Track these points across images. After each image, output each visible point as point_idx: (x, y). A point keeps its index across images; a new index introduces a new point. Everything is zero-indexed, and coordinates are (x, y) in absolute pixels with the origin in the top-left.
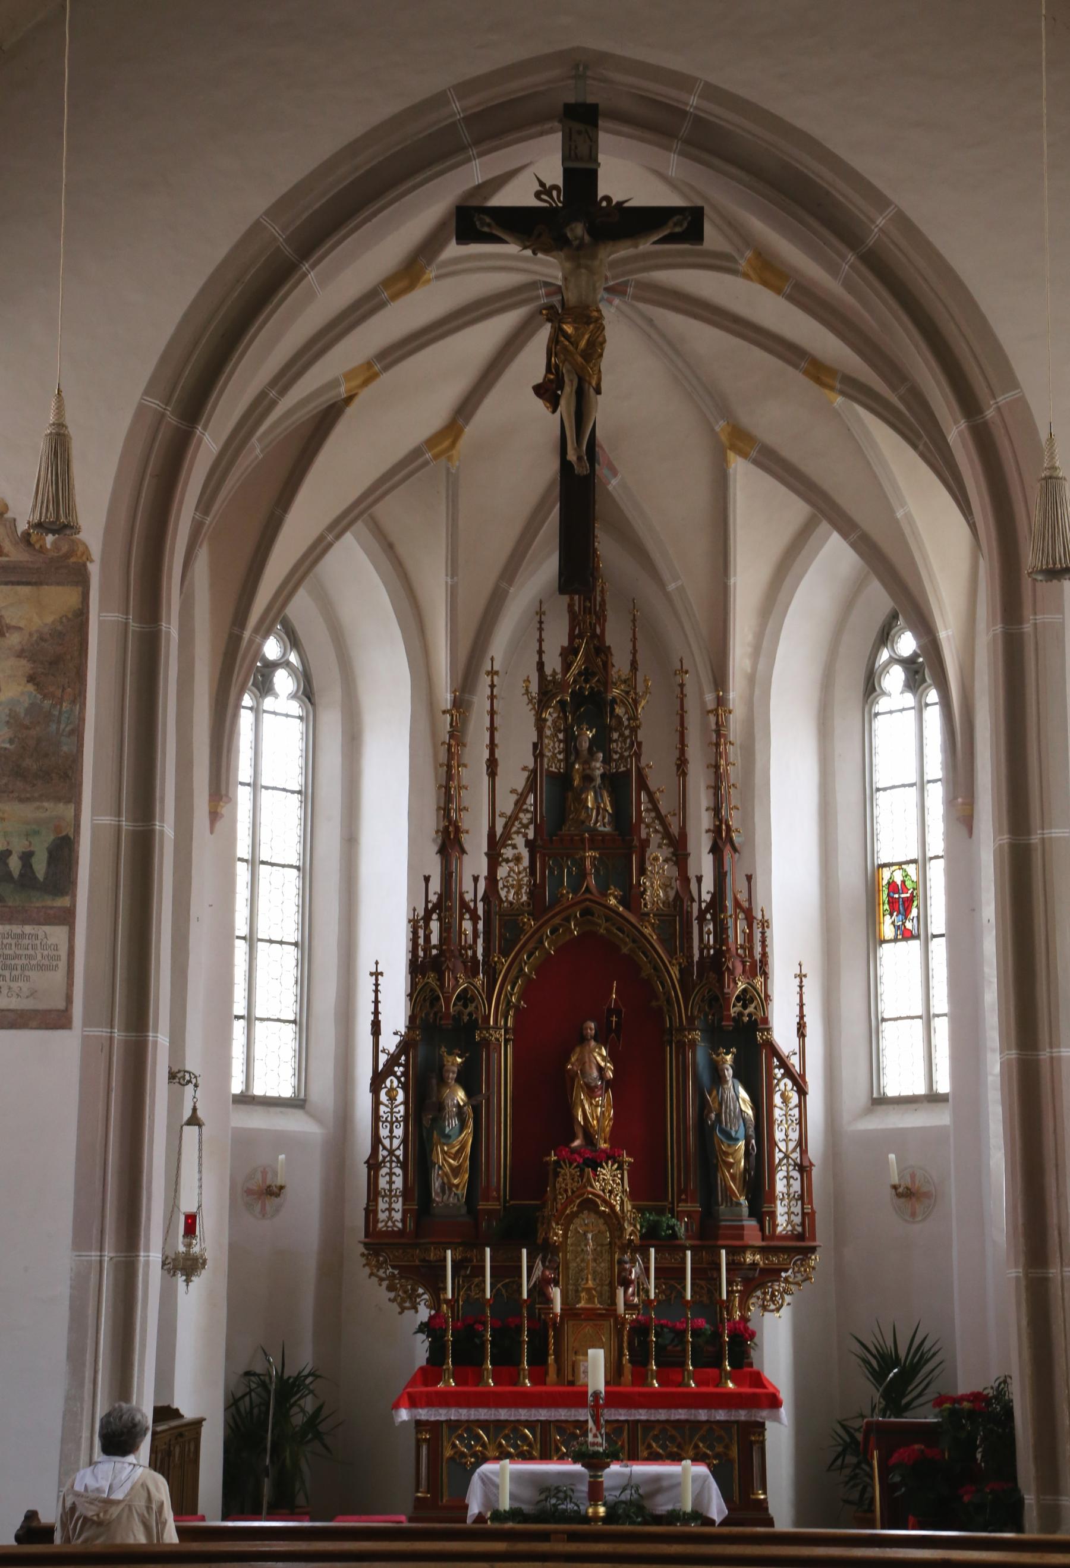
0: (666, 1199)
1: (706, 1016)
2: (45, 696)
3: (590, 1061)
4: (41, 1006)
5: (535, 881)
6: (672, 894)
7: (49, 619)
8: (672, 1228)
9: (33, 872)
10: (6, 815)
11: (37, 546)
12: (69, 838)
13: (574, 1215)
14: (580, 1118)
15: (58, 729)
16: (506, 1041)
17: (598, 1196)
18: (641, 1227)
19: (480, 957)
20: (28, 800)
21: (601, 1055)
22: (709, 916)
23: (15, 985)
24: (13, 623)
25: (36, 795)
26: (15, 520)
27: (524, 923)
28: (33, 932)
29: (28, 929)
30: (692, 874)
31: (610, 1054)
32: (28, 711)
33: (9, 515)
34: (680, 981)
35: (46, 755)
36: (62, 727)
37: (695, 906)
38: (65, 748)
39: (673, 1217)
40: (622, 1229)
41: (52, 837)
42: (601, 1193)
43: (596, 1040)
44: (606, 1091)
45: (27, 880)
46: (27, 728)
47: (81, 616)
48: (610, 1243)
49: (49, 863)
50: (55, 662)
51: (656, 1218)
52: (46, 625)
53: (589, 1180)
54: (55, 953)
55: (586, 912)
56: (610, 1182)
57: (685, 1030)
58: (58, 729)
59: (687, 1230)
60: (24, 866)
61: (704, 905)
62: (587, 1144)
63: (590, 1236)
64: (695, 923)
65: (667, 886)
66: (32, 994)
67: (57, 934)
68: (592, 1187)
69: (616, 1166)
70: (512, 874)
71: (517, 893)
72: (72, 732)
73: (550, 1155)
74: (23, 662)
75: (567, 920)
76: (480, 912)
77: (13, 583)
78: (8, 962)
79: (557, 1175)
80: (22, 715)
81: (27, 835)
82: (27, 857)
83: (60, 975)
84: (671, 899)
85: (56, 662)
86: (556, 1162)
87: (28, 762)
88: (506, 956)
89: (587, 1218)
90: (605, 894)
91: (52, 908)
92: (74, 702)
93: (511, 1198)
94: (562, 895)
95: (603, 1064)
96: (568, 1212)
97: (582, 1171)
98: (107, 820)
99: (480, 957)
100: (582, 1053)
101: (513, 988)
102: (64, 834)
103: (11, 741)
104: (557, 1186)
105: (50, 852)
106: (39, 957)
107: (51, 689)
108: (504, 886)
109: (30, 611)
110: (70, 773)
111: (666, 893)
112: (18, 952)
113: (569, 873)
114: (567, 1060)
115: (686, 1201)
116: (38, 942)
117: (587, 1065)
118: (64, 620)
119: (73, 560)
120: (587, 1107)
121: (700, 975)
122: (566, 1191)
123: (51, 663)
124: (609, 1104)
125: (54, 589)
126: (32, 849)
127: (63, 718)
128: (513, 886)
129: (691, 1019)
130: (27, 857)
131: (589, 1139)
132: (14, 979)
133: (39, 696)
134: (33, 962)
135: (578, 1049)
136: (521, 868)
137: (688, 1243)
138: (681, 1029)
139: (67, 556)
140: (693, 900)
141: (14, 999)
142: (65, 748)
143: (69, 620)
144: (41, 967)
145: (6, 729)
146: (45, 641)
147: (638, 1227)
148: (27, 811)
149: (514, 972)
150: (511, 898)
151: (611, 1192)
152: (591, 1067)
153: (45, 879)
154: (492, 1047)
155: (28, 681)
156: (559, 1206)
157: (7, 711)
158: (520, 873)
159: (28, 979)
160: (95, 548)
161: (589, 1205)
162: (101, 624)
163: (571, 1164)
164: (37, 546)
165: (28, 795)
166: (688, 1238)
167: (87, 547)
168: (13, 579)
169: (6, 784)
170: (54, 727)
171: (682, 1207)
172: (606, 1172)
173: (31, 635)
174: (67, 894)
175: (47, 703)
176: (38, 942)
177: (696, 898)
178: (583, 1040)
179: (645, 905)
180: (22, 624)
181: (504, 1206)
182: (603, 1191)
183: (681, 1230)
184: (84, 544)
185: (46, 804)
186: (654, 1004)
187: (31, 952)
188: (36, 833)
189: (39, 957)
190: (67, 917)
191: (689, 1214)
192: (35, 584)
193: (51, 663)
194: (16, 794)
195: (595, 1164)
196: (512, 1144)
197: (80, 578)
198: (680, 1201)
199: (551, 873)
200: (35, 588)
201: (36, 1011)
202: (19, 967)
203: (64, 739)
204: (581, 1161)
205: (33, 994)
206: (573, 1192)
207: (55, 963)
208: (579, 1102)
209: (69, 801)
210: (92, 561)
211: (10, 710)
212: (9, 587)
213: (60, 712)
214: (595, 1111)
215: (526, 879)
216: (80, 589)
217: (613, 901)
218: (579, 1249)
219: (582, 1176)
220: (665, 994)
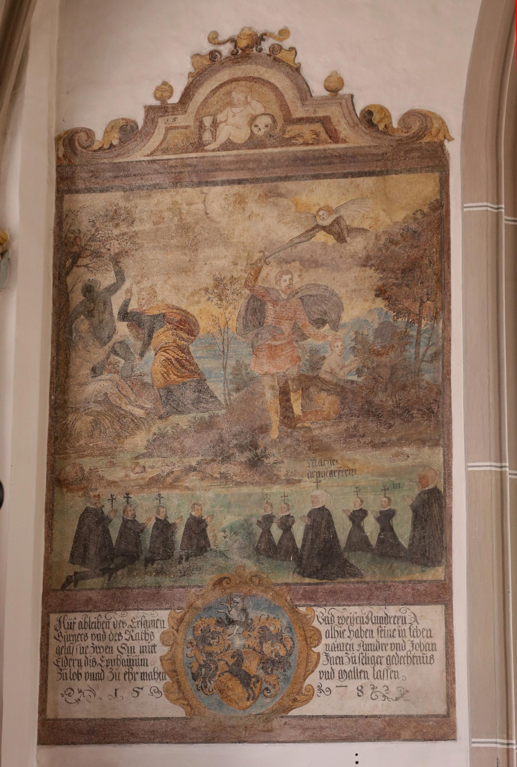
2: (399, 313)
4: (414, 711)
7: (400, 216)
9: (395, 537)
10: (357, 466)
11: (381, 127)
12: (439, 492)
15: (417, 354)
20: (383, 444)
23: (379, 683)
24: (356, 225)
25: (394, 438)
26: (352, 96)
28: (398, 614)
29: (392, 610)
32: (379, 333)
33: (345, 91)
35: (404, 387)
36: (422, 350)
38: (427, 377)
41: (417, 491)
45: (387, 548)
46: (379, 354)
47: (440, 208)
49: (414, 526)
50: (410, 269)
52: (396, 223)
54: (429, 641)
58: (417, 354)
60: (382, 530)
66: (402, 695)
67: (430, 616)
72: (435, 356)
74: (370, 271)
77: (353, 175)
78: (370, 654)
80: (372, 338)
81: (385, 489)
82: (386, 518)
83: (436, 669)
85: (412, 269)
87: (380, 398)
91: (421, 582)
92: (435, 318)
98: (487, 466)
102: (431, 486)
103: (359, 372)
105: (415, 510)
106: (409, 647)
107: (407, 303)
109: (377, 207)
110: (435, 408)
112: (382, 641)
116: (406, 627)
118: (419, 216)
119: (426, 139)
123: (403, 271)
125: (403, 177)
126: (392, 507)
127: (423, 340)
130: (386, 518)
132: (379, 676)
133: (392, 314)
134: (401, 653)
139: (418, 136)
141: (380, 702)
142: (427, 377)
143: (424, 215)
144: (412, 660)
145: (352, 357)
146: (397, 243)
148: (383, 459)
153: (410, 545)
155: (377, 296)
157: (352, 335)
159: (396, 675)
160: (455, 124)
162: (465, 216)
164: (381, 127)
165: (384, 439)
167: (443, 122)
168: (352, 170)
169: (355, 427)
170: (411, 351)
173: (377, 237)
174: (439, 563)
175: (401, 322)
176: (406, 627)
180: (366, 225)
184: (440, 118)
185: (406, 450)
187: (397, 640)
188: (397, 486)
189: (409, 647)
190: (441, 594)
192: (380, 173)
193: (403, 271)
194: (368, 439)
197: (436, 160)
200: (380, 178)
201: (409, 717)
202: (384, 661)
203: (424, 365)
205: (403, 694)
207: (429, 654)
209: (436, 444)
210: (450, 139)
211: (356, 333)
212: (349, 180)
213: (419, 332)
216: (437, 174)
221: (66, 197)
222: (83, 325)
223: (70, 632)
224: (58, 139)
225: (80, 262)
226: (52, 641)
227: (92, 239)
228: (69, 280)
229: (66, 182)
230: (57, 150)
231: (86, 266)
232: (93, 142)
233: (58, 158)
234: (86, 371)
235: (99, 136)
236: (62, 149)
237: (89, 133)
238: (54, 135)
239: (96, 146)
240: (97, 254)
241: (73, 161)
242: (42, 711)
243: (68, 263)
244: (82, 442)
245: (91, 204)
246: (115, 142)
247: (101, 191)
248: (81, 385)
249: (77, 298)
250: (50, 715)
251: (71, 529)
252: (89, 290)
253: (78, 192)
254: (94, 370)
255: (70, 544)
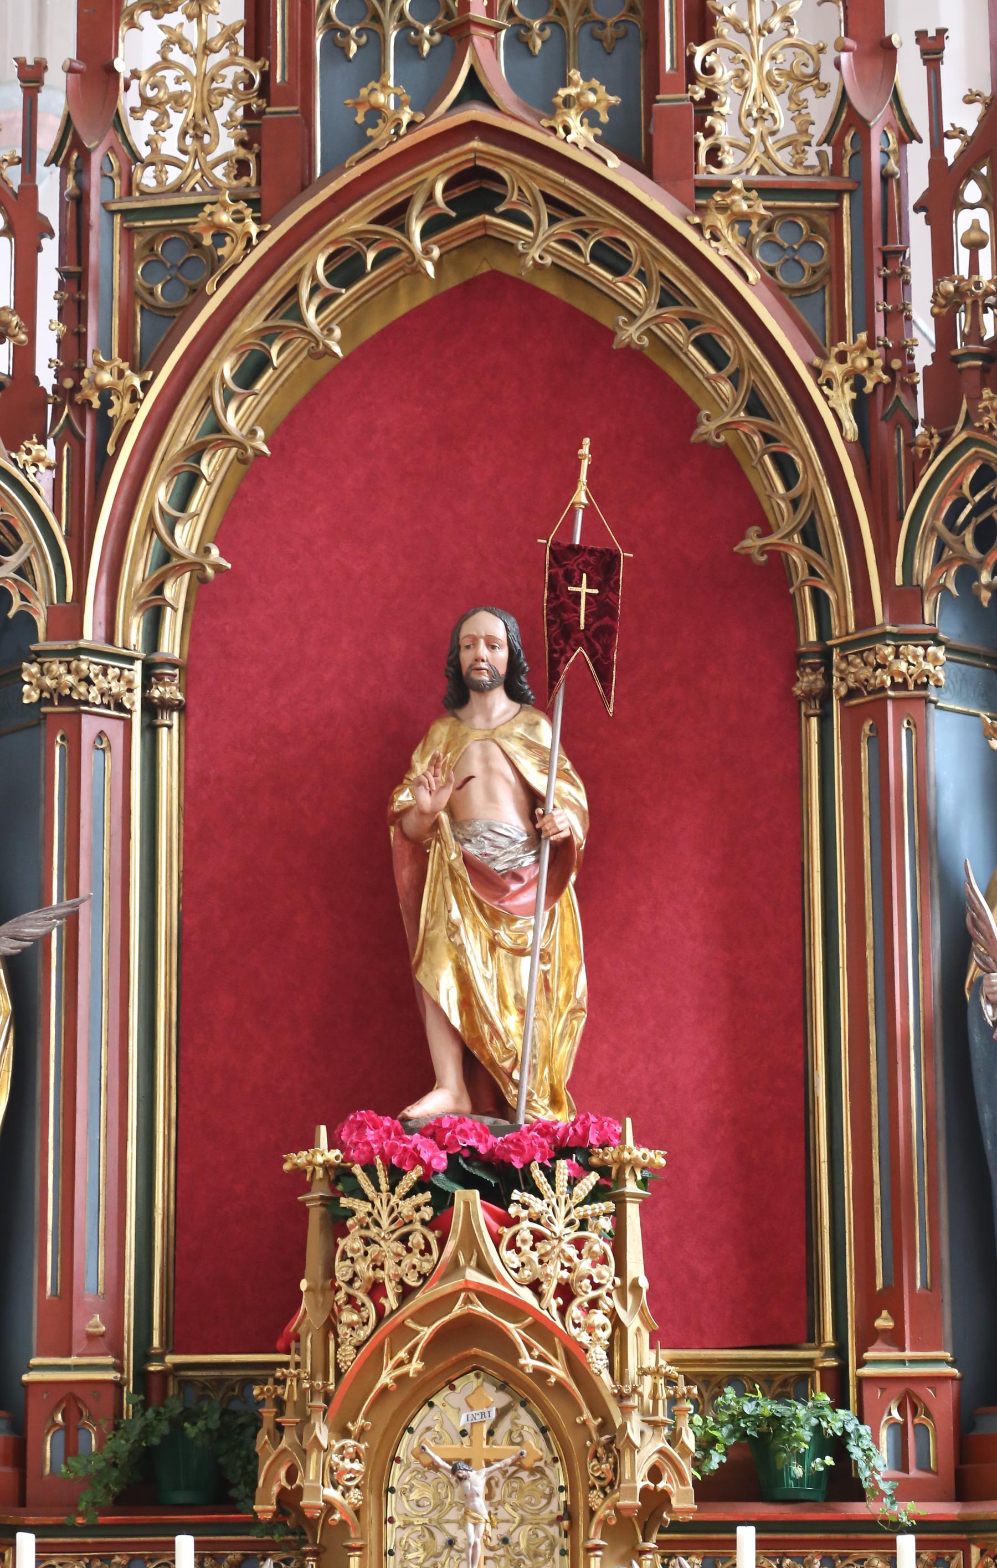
0: (811, 1336)
1: (968, 575)
3: (489, 770)
5: (267, 76)
6: (821, 111)
8: (837, 1445)
13: (419, 1393)
14: (446, 994)
16: (151, 709)
17: (514, 1310)
18: (706, 1444)
19: (46, 378)
21: (531, 746)
22: (972, 192)
27: (220, 234)
30: (901, 31)
31: (568, 741)
34: (864, 448)
37: (918, 157)
39: (840, 1402)
40: (614, 1445)
42: (527, 1296)
43: (514, 693)
44: (555, 890)
48: (569, 1513)
51: (769, 1408)
53: (470, 1242)
55: (476, 190)
56: (577, 1261)
57: (883, 637)
59: (901, 1462)
61: (952, 149)
62: (477, 1109)
63: (477, 1479)
64: (919, 233)
65: (803, 81)
68: (483, 1267)
69: (592, 1179)
70: (176, 55)
71: (195, 130)
73: (309, 1143)
75: (395, 216)
76: (49, 204)
79: (337, 1224)
84: (818, 131)
86: (339, 1176)
88: (146, 362)
89: (464, 1408)
90: (548, 108)
93: (173, 1343)
94: (376, 113)
95: (538, 782)
96: (386, 1378)
97: (442, 1201)
99: (46, 378)
100: (455, 742)
101: (183, 502)
104: (342, 1270)
108: (147, 103)
111: (798, 106)
113: (409, 47)
114: (398, 772)
115: (895, 1339)
117: (476, 789)
120: (474, 948)
121: (942, 417)
122: (376, 1290)
124: (565, 950)
128: (177, 101)
129: (906, 600)
131: (487, 1087)
135: (441, 731)
136: (214, 29)
137: (907, 1510)
138: (866, 639)
140: (908, 134)
147: (689, 1440)
149: (181, 433)
150: (169, 147)
151: (566, 1292)
152: (491, 796)
154: (89, 726)
156: (347, 1353)
158: (207, 49)
161: (468, 1345)
163: (396, 1175)
166: (904, 1492)
171: (881, 1362)
172: (555, 1203)
177: (921, 124)
178: (460, 691)
179: (714, 156)
181: (142, 1376)
182: (535, 1286)
183: (875, 1458)
186: (752, 542)
191: (909, 1394)
195: (500, 1180)
196: (182, 1123)
198: (868, 1337)
199: (336, 47)
204: (440, 1161)
206: (406, 1293)
208: (441, 932)
214: (512, 980)
215: (231, 72)
217: (581, 133)
218: (441, 1539)
219: (441, 1223)
220: (795, 503)
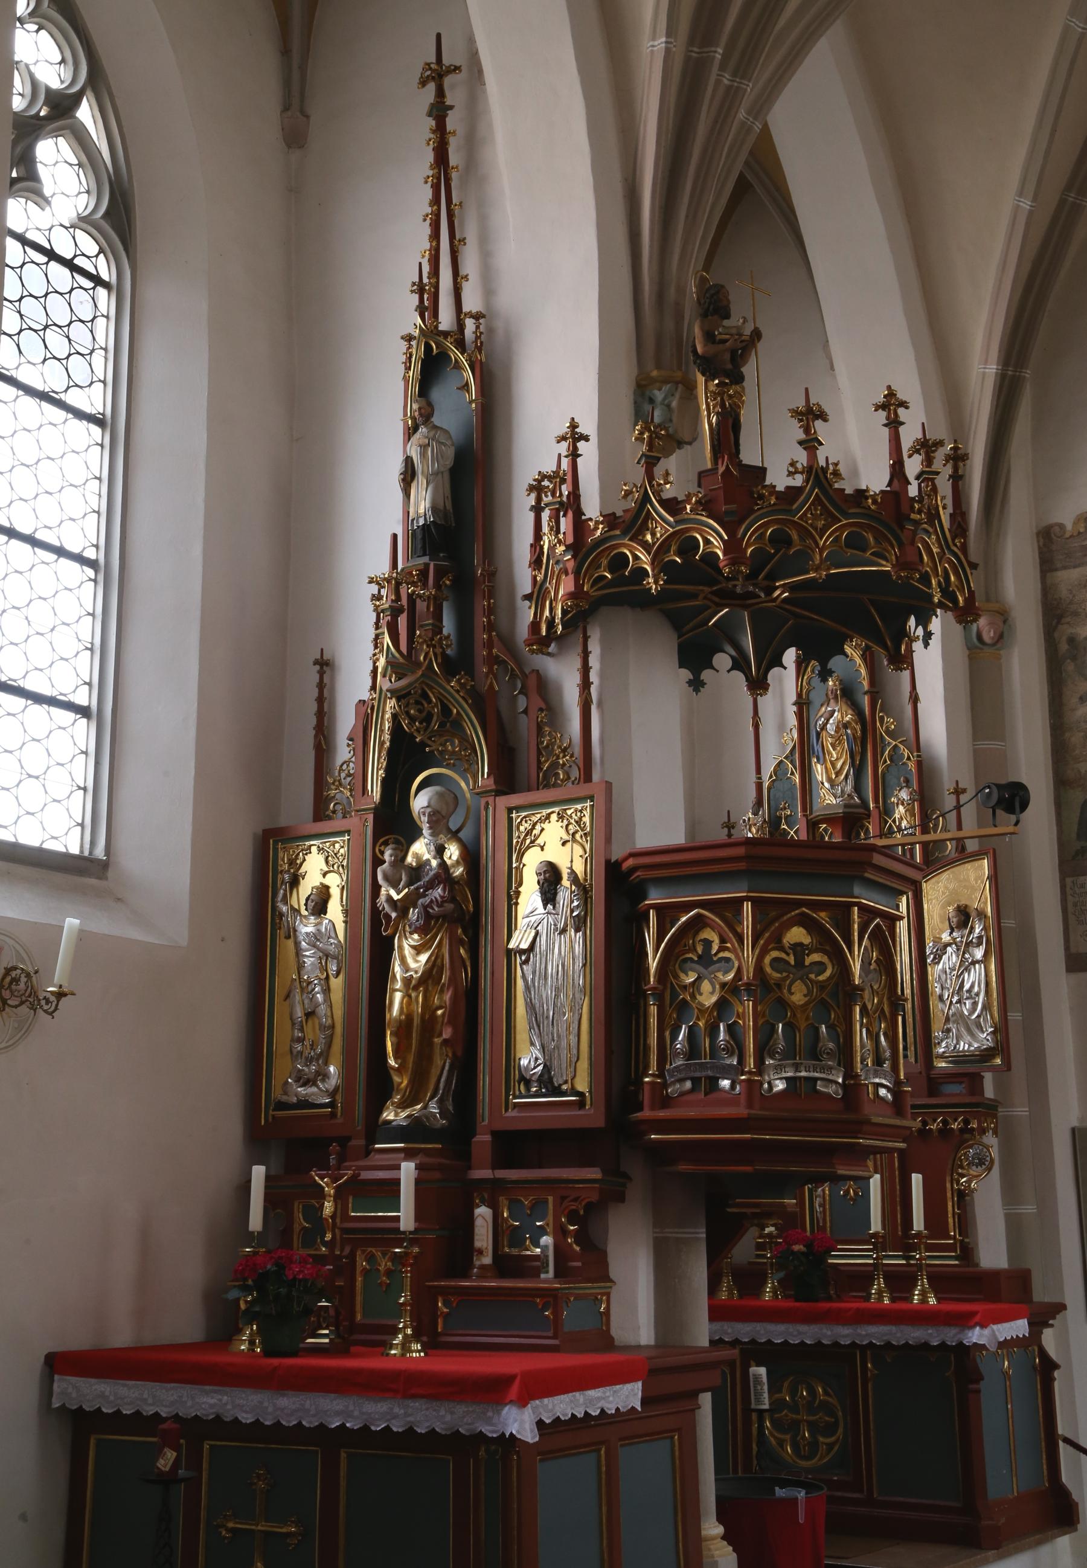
221: (1048, 574)
222: (1070, 667)
223: (1082, 890)
224: (1038, 534)
225: (1063, 620)
226: (1070, 898)
227: (1071, 603)
228: (1056, 635)
229: (1047, 563)
230: (1038, 541)
231: (1068, 623)
232: (1065, 533)
233: (1039, 548)
234: (1075, 700)
235: (1069, 526)
236: (1042, 540)
237: (1061, 526)
238: (1035, 531)
239: (1067, 535)
240: (1076, 614)
241: (1050, 546)
242: (1067, 948)
243: (1054, 623)
244: (1077, 752)
245: (1068, 578)
246: (1082, 530)
247: (1075, 567)
248: (1073, 710)
249: (1064, 647)
250: (1073, 950)
251: (1075, 816)
252: (1072, 640)
253: (1056, 570)
254: (1081, 698)
255: (1075, 827)
